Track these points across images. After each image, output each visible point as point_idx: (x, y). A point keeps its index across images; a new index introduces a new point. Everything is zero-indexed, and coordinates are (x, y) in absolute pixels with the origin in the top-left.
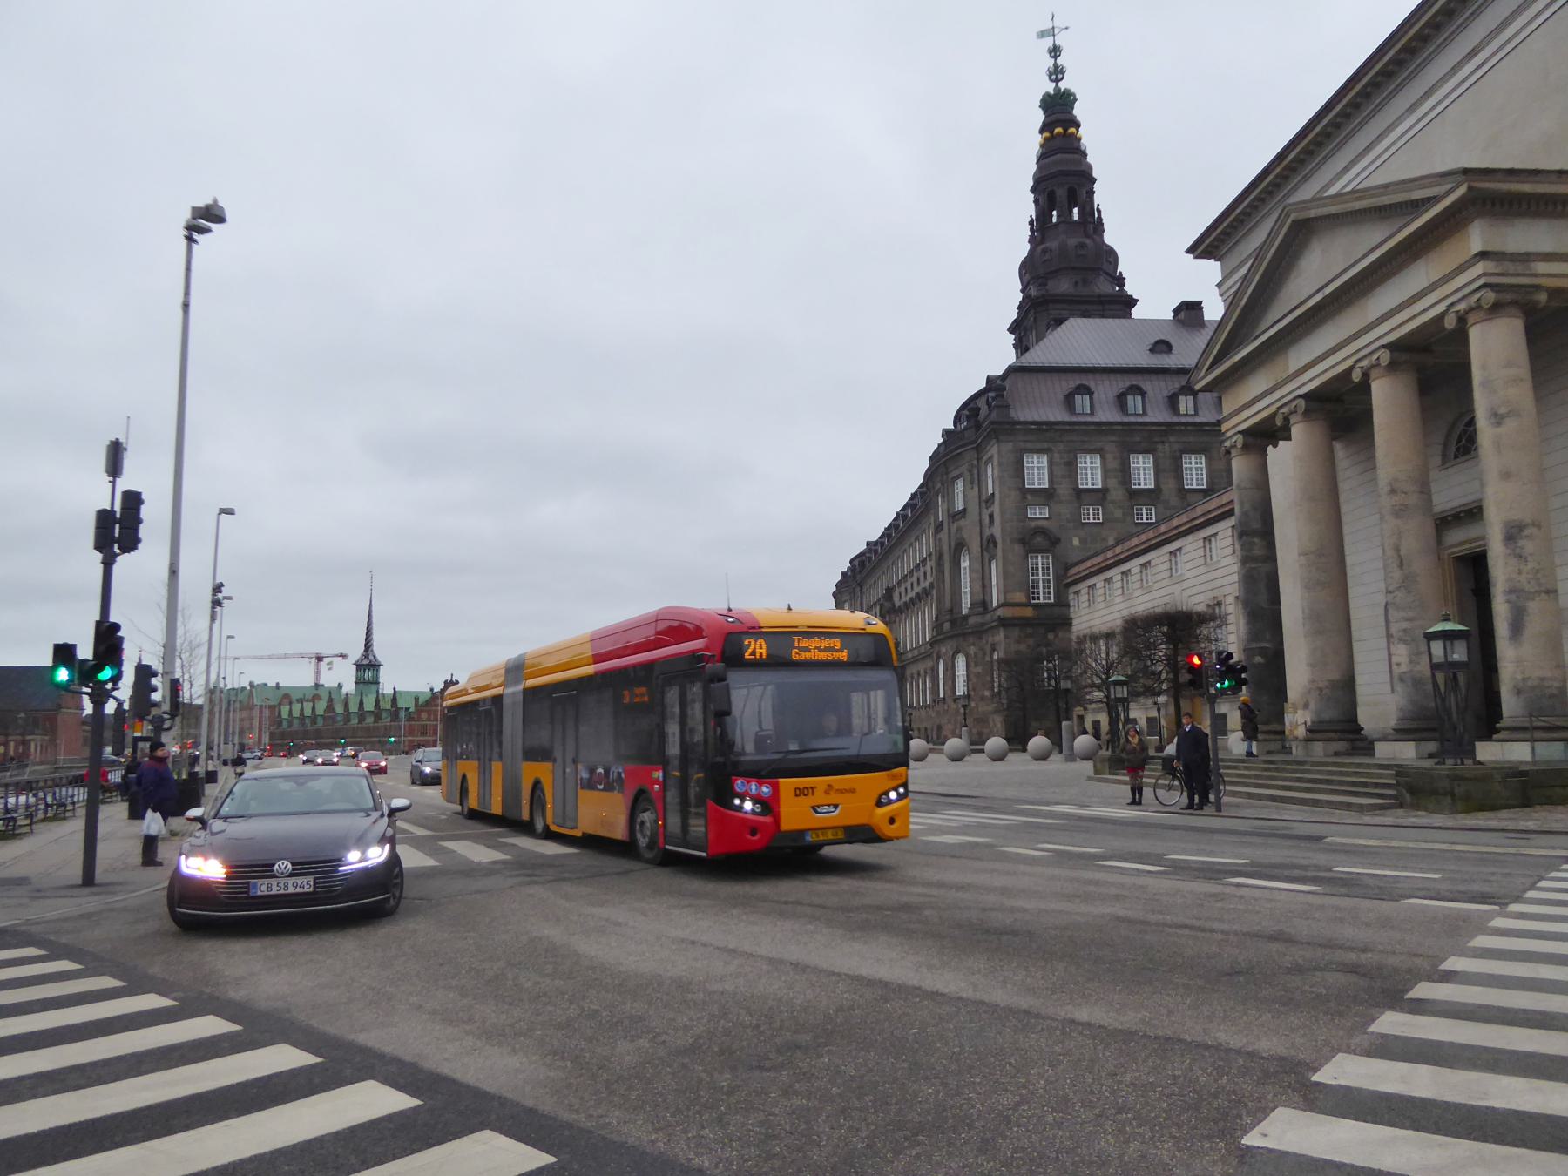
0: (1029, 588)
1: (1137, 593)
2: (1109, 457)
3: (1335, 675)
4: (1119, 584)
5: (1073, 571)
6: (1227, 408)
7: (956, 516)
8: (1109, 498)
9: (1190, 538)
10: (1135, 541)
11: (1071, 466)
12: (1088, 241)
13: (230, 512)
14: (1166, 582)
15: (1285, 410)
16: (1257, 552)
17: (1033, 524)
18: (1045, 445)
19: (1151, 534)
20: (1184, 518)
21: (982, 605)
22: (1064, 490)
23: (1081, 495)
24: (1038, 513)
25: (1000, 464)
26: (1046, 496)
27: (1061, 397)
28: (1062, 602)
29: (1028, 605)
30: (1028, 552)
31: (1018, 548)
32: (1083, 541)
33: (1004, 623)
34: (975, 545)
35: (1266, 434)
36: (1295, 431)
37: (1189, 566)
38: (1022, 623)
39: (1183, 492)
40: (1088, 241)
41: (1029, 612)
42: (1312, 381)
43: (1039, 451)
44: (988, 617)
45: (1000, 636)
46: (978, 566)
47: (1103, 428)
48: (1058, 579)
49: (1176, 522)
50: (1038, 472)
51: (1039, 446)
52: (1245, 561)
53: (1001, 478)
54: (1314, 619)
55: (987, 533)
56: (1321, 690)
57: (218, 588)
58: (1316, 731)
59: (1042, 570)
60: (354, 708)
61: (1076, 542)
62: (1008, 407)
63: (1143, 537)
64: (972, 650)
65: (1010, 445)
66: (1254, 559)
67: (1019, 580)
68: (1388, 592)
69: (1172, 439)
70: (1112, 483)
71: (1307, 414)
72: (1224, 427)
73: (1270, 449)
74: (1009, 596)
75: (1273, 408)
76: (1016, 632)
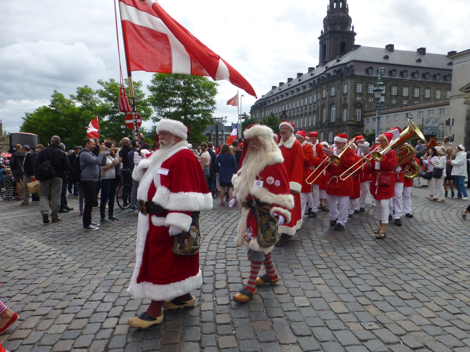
0: (355, 117)
11: (367, 87)
12: (345, 15)
18: (362, 82)
21: (339, 119)
22: (365, 93)
24: (358, 98)
26: (361, 94)
27: (365, 69)
28: (362, 121)
29: (355, 121)
31: (354, 107)
32: (368, 106)
34: (338, 105)
38: (353, 125)
39: (391, 96)
40: (345, 15)
41: (355, 123)
43: (360, 83)
44: (342, 123)
45: (348, 127)
48: (362, 115)
50: (359, 88)
61: (366, 106)
62: (354, 71)
64: (336, 131)
65: (353, 81)
76: (352, 128)
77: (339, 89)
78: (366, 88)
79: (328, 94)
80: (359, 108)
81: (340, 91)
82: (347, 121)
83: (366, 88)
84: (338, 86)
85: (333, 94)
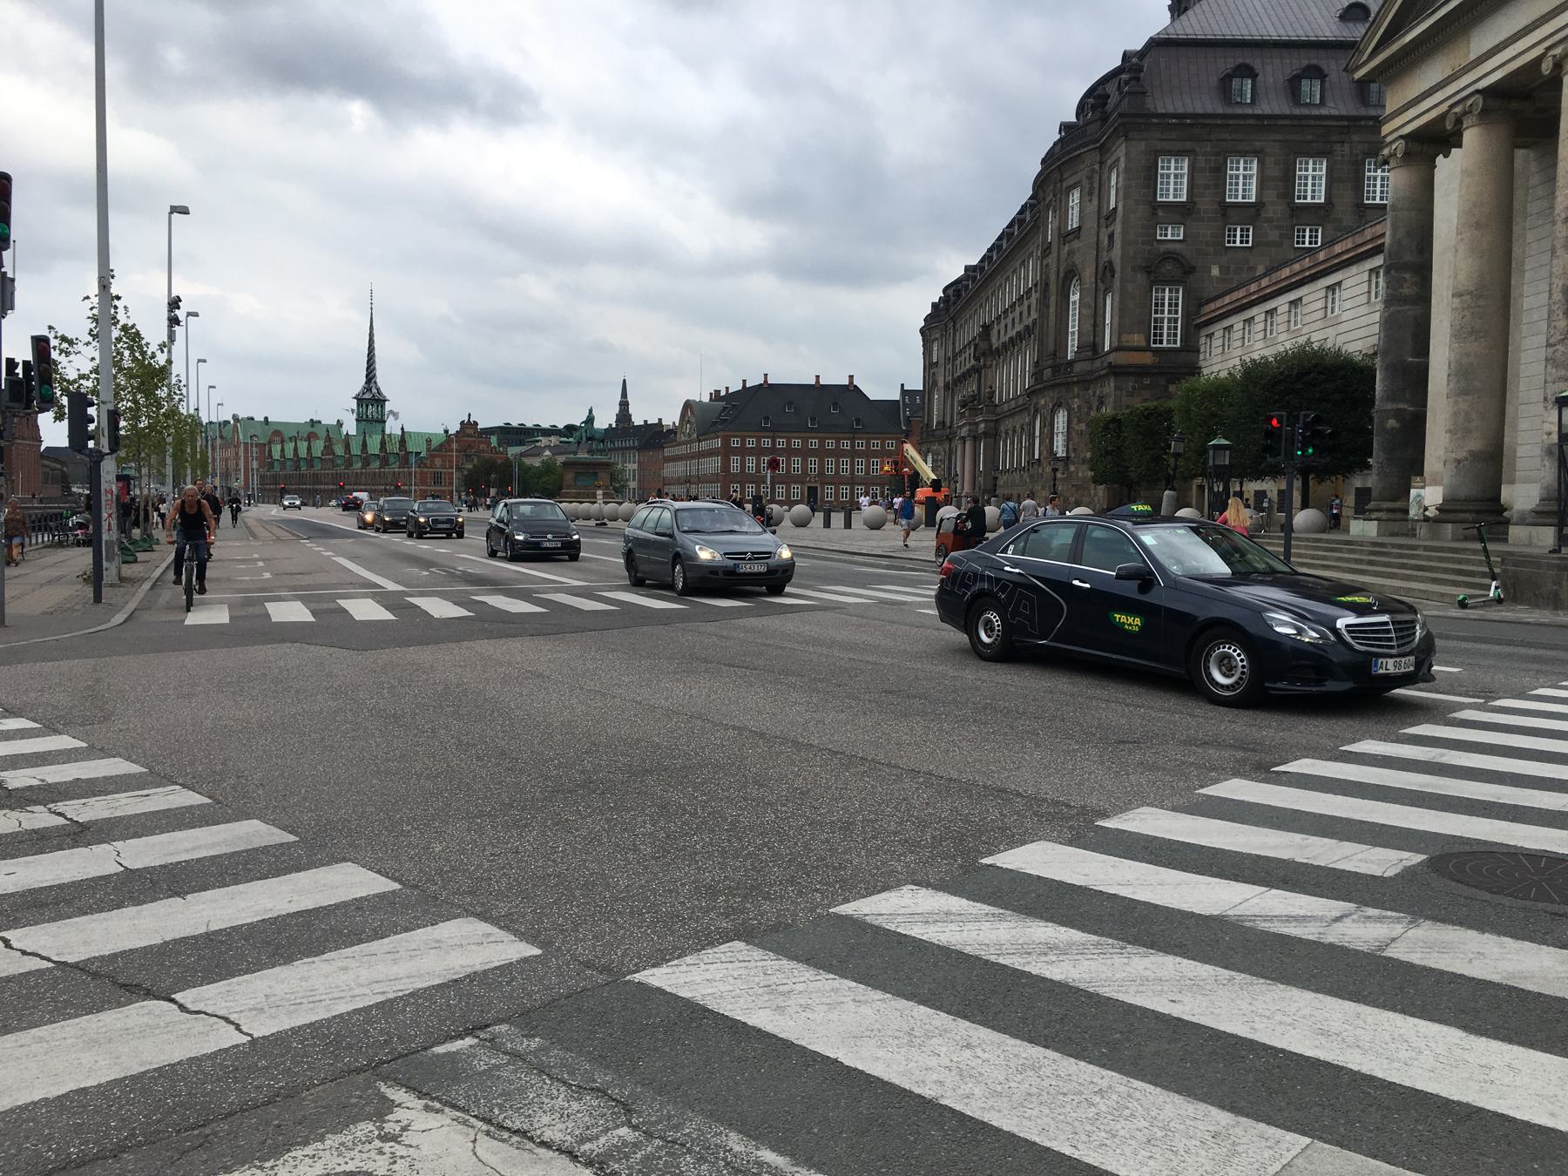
1: (1282, 337)
2: (1270, 161)
3: (1475, 444)
4: (1261, 326)
5: (1207, 308)
6: (1392, 102)
7: (1067, 236)
8: (1264, 215)
9: (1354, 269)
10: (1286, 272)
11: (1219, 171)
13: (184, 211)
14: (1319, 324)
15: (1457, 109)
16: (1406, 290)
17: (1162, 248)
18: (1188, 145)
19: (1307, 262)
20: (1349, 244)
21: (1091, 347)
22: (1206, 204)
23: (1229, 213)
24: (1173, 234)
25: (1127, 170)
26: (1182, 212)
27: (1214, 80)
28: (1191, 347)
29: (1147, 349)
30: (1153, 283)
31: (1141, 278)
33: (1117, 371)
34: (1088, 273)
35: (1435, 140)
36: (1471, 136)
37: (1348, 305)
38: (1139, 372)
41: (1147, 359)
42: (1492, 73)
43: (1179, 153)
44: (1097, 364)
46: (1090, 300)
47: (1267, 124)
48: (1187, 316)
49: (1338, 248)
50: (1174, 181)
51: (1179, 146)
52: (1389, 302)
53: (1126, 187)
54: (1462, 373)
55: (1105, 257)
56: (1459, 462)
57: (174, 303)
58: (1448, 510)
59: (1169, 306)
60: (356, 450)
61: (1215, 271)
63: (1297, 267)
64: (1076, 403)
65: (1142, 146)
66: (1404, 300)
67: (1138, 318)
68: (1549, 345)
69: (1356, 138)
70: (1270, 195)
71: (1485, 114)
72: (1386, 129)
73: (1440, 159)
74: (1125, 338)
75: (1444, 107)
76: (1130, 383)
77: (1091, 194)
78: (1210, 178)
79: (1056, 224)
80: (1171, 282)
81: (1095, 202)
82: (1113, 350)
83: (1210, 178)
84: (1090, 178)
85: (1073, 222)
